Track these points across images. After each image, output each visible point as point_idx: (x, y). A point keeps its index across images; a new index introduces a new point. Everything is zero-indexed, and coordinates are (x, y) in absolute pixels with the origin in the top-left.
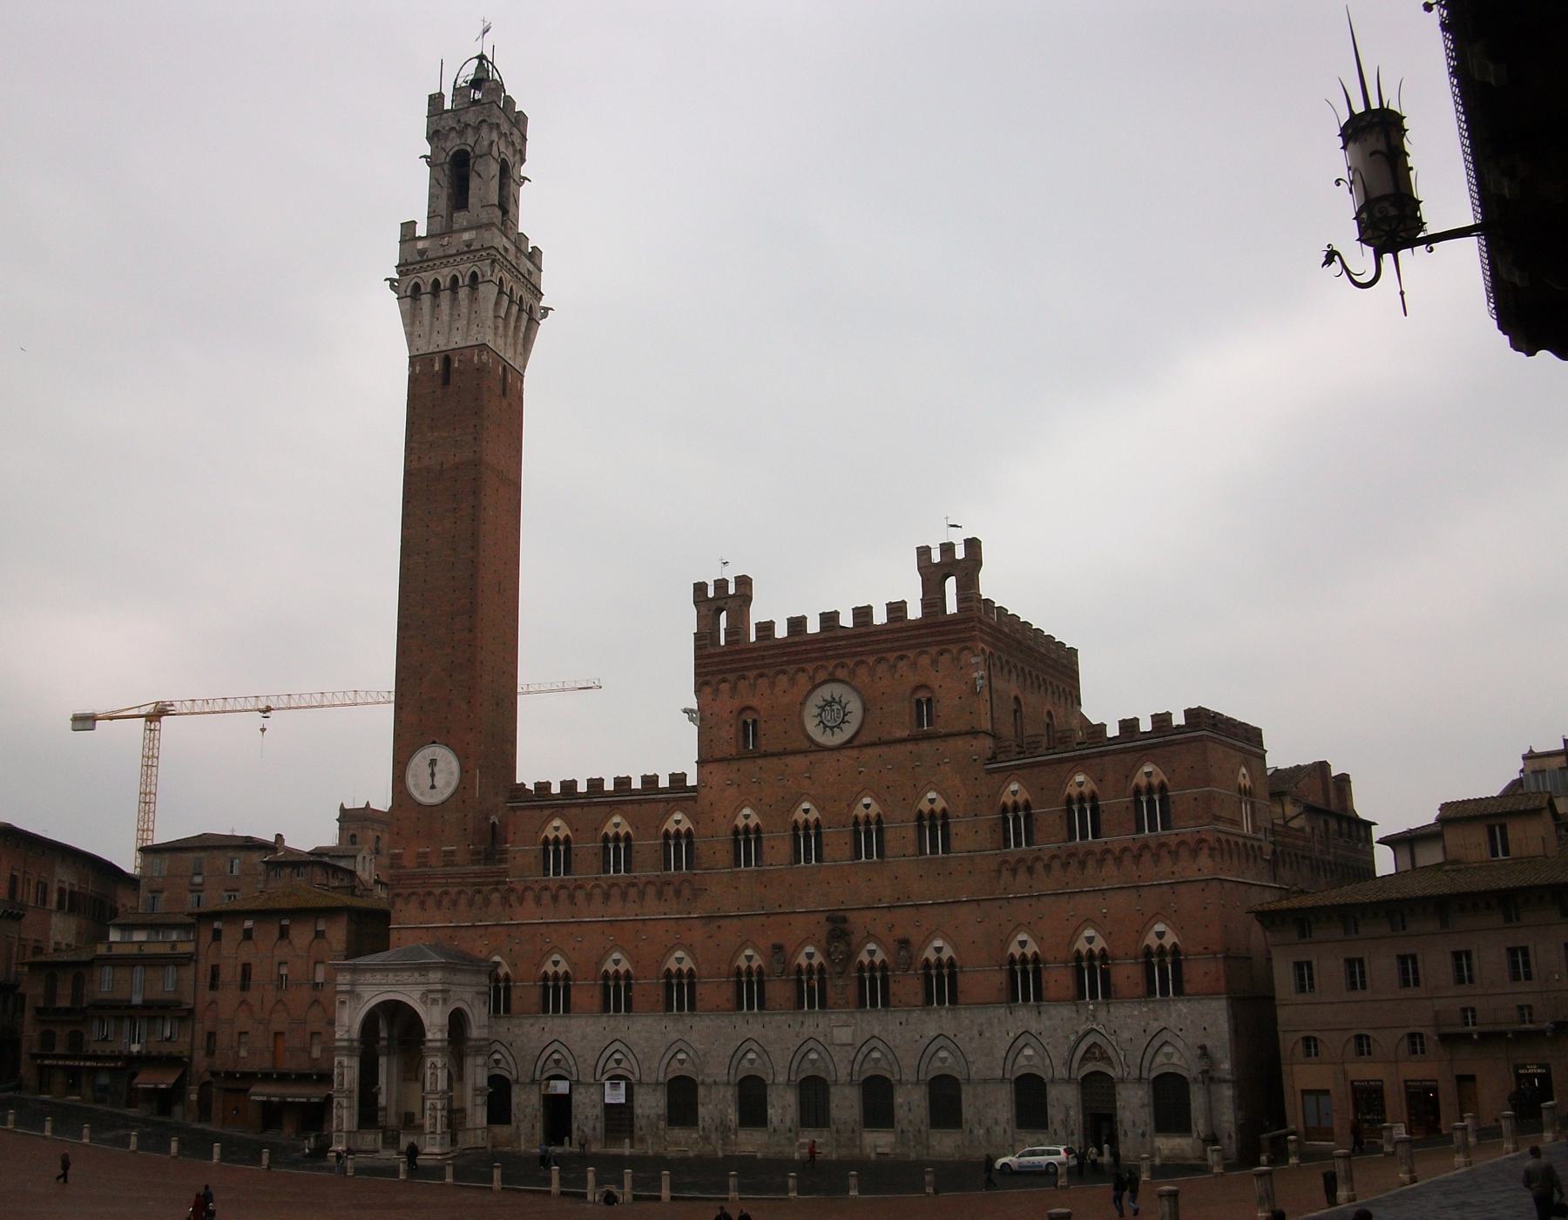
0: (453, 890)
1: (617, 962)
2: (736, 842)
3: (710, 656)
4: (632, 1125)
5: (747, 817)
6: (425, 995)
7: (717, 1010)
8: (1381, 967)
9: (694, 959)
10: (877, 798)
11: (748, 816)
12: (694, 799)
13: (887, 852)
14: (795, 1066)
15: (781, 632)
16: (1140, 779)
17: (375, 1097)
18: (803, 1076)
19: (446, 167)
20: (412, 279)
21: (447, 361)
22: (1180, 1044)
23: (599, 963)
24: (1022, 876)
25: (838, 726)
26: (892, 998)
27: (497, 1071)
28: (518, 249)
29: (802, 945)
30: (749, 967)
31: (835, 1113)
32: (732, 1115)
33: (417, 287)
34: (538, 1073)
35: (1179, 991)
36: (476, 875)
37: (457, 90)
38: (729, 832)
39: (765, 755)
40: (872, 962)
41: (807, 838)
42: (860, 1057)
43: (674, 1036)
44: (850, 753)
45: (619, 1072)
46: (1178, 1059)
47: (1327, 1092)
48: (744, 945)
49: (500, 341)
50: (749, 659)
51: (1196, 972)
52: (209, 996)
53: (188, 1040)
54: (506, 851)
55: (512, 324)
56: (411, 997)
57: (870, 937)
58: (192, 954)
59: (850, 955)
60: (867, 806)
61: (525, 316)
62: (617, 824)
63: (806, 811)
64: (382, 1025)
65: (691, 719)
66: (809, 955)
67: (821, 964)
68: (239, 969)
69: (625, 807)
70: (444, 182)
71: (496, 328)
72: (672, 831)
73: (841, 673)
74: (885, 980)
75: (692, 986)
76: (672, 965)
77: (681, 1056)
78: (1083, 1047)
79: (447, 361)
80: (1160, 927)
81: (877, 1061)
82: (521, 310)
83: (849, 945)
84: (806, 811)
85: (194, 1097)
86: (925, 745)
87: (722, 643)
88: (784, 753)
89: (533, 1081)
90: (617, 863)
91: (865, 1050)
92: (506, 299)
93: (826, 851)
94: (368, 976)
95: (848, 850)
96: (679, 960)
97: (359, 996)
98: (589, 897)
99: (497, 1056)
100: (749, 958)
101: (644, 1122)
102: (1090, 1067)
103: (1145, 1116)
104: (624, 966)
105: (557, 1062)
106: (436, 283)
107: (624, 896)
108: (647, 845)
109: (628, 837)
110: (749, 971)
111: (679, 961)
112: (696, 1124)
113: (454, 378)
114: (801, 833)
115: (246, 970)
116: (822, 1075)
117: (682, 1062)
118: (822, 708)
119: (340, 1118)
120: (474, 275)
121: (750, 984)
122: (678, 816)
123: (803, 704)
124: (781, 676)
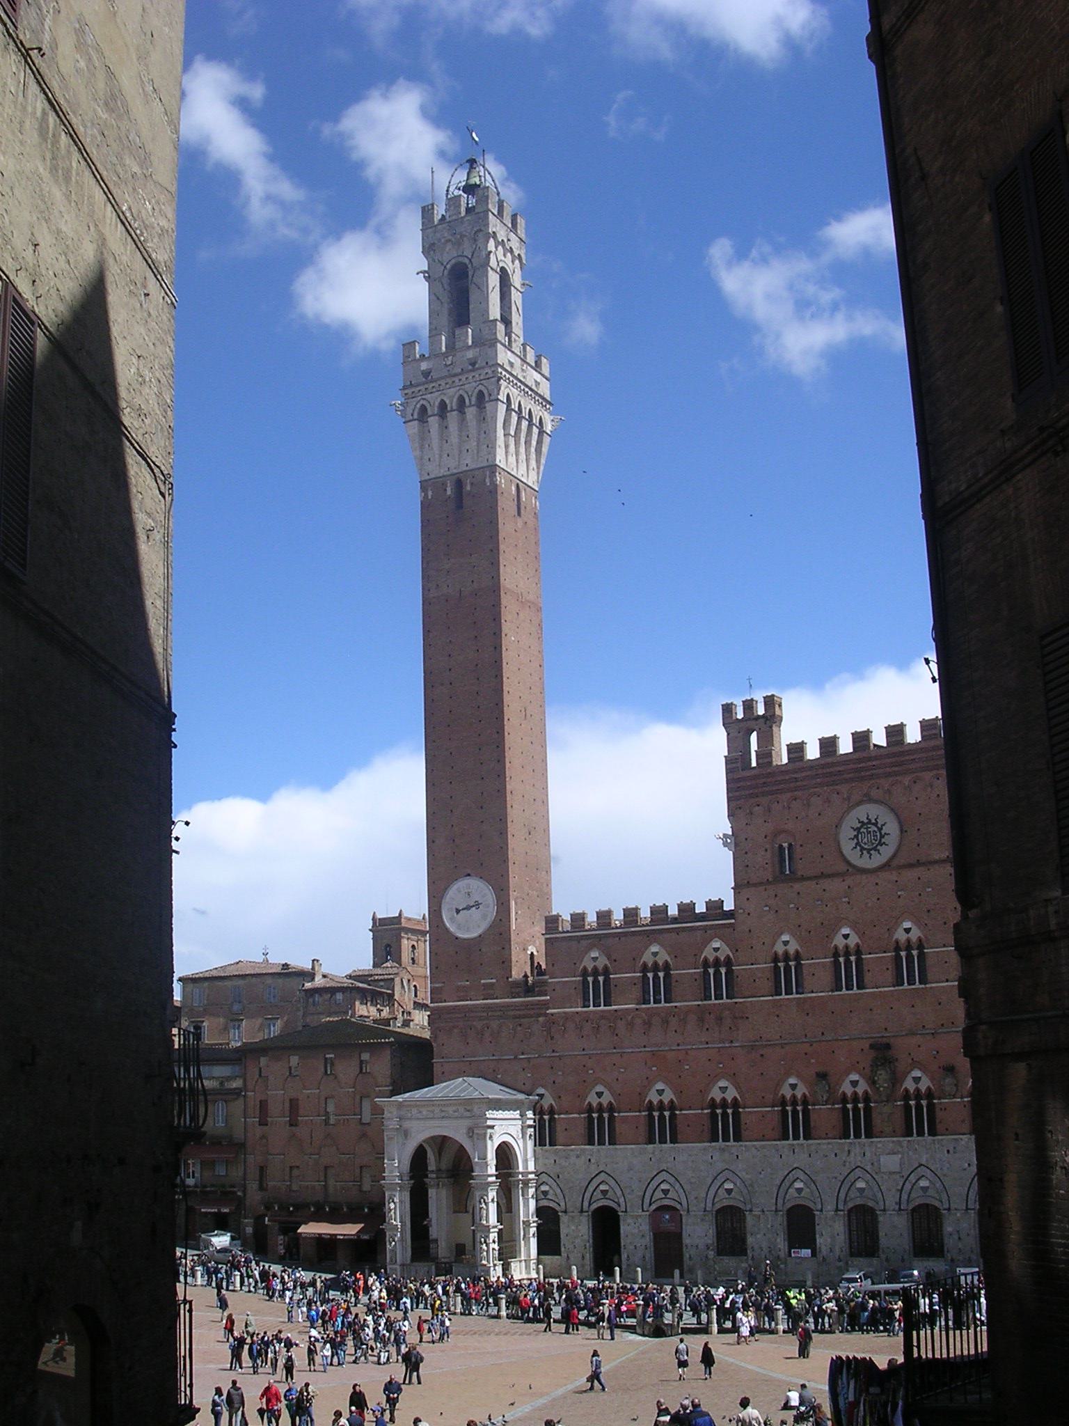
0: (494, 1024)
1: (660, 1092)
2: (777, 968)
3: (739, 780)
4: (681, 1255)
5: (786, 943)
6: (471, 1132)
7: (763, 1138)
9: (738, 1088)
10: (917, 922)
11: (787, 942)
13: (930, 976)
14: (842, 1195)
15: (813, 753)
17: (426, 1229)
18: (850, 1205)
19: (445, 281)
20: (415, 405)
21: (459, 484)
23: (642, 1095)
25: (875, 849)
26: (939, 1126)
27: (544, 1203)
28: (524, 361)
30: (794, 1096)
31: (883, 1241)
32: (781, 1243)
33: (423, 410)
34: (586, 1204)
36: (515, 1007)
37: (453, 202)
38: (769, 959)
39: (803, 879)
40: (917, 1090)
41: (848, 969)
42: (908, 1186)
43: (720, 1166)
44: (884, 875)
45: (666, 1202)
48: (788, 1075)
49: (512, 459)
52: (259, 1131)
53: (241, 1174)
54: (545, 983)
55: (523, 440)
56: (456, 1131)
57: (915, 1064)
58: (240, 1090)
59: (896, 1080)
61: (535, 430)
62: (656, 952)
63: (845, 936)
64: (431, 1156)
65: (725, 844)
66: (853, 1083)
67: (866, 1092)
68: (287, 1105)
69: (665, 935)
70: (445, 298)
71: (507, 447)
72: (711, 959)
73: (874, 793)
74: (931, 1107)
75: (736, 1115)
76: (716, 1094)
77: (728, 1186)
79: (459, 484)
81: (925, 1189)
82: (531, 424)
83: (894, 1073)
84: (846, 936)
85: (249, 1230)
87: (754, 764)
88: (822, 876)
89: (582, 1211)
90: (657, 992)
91: (913, 1178)
92: (514, 417)
93: (868, 978)
94: (414, 1111)
95: (889, 976)
96: (723, 1089)
97: (406, 1134)
98: (631, 1024)
99: (544, 1188)
100: (793, 1087)
101: (693, 1252)
104: (668, 1096)
105: (604, 1192)
106: (443, 405)
107: (666, 1022)
108: (686, 973)
109: (667, 967)
110: (794, 1102)
111: (723, 1090)
112: (743, 1252)
113: (467, 502)
114: (841, 959)
115: (294, 1105)
116: (871, 1204)
117: (729, 1191)
118: (858, 829)
119: (394, 1251)
120: (481, 392)
121: (795, 1112)
122: (716, 944)
124: (814, 800)
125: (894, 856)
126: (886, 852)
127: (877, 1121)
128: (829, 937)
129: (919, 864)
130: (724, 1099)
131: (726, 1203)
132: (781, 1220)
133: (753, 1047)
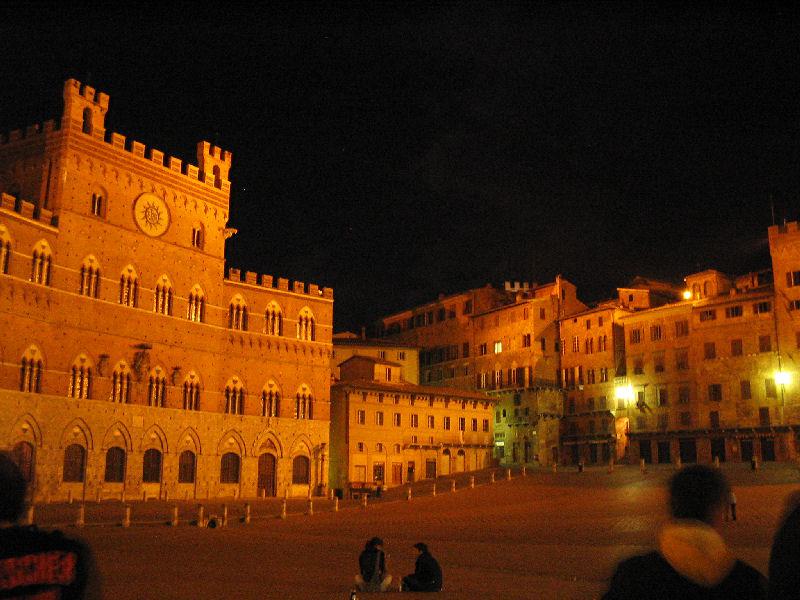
5: (91, 261)
8: (389, 418)
9: (44, 353)
11: (92, 261)
12: (55, 234)
13: (174, 311)
16: (302, 313)
22: (308, 442)
24: (237, 345)
26: (168, 403)
29: (118, 359)
31: (128, 473)
32: (61, 472)
35: (311, 418)
39: (109, 222)
41: (131, 289)
46: (301, 448)
47: (365, 467)
50: (106, 154)
51: (317, 408)
57: (162, 364)
59: (149, 369)
60: (164, 280)
63: (129, 271)
69: (13, 223)
77: (26, 426)
78: (263, 440)
80: (305, 386)
81: (154, 440)
86: (198, 255)
93: (140, 302)
96: (33, 352)
100: (83, 360)
102: (265, 451)
103: (290, 475)
111: (33, 353)
117: (25, 430)
123: (135, 201)
125: (163, 234)
126: (161, 230)
127: (134, 392)
128: (120, 268)
129: (175, 244)
130: (32, 360)
131: (23, 439)
132: (62, 453)
133: (58, 325)
